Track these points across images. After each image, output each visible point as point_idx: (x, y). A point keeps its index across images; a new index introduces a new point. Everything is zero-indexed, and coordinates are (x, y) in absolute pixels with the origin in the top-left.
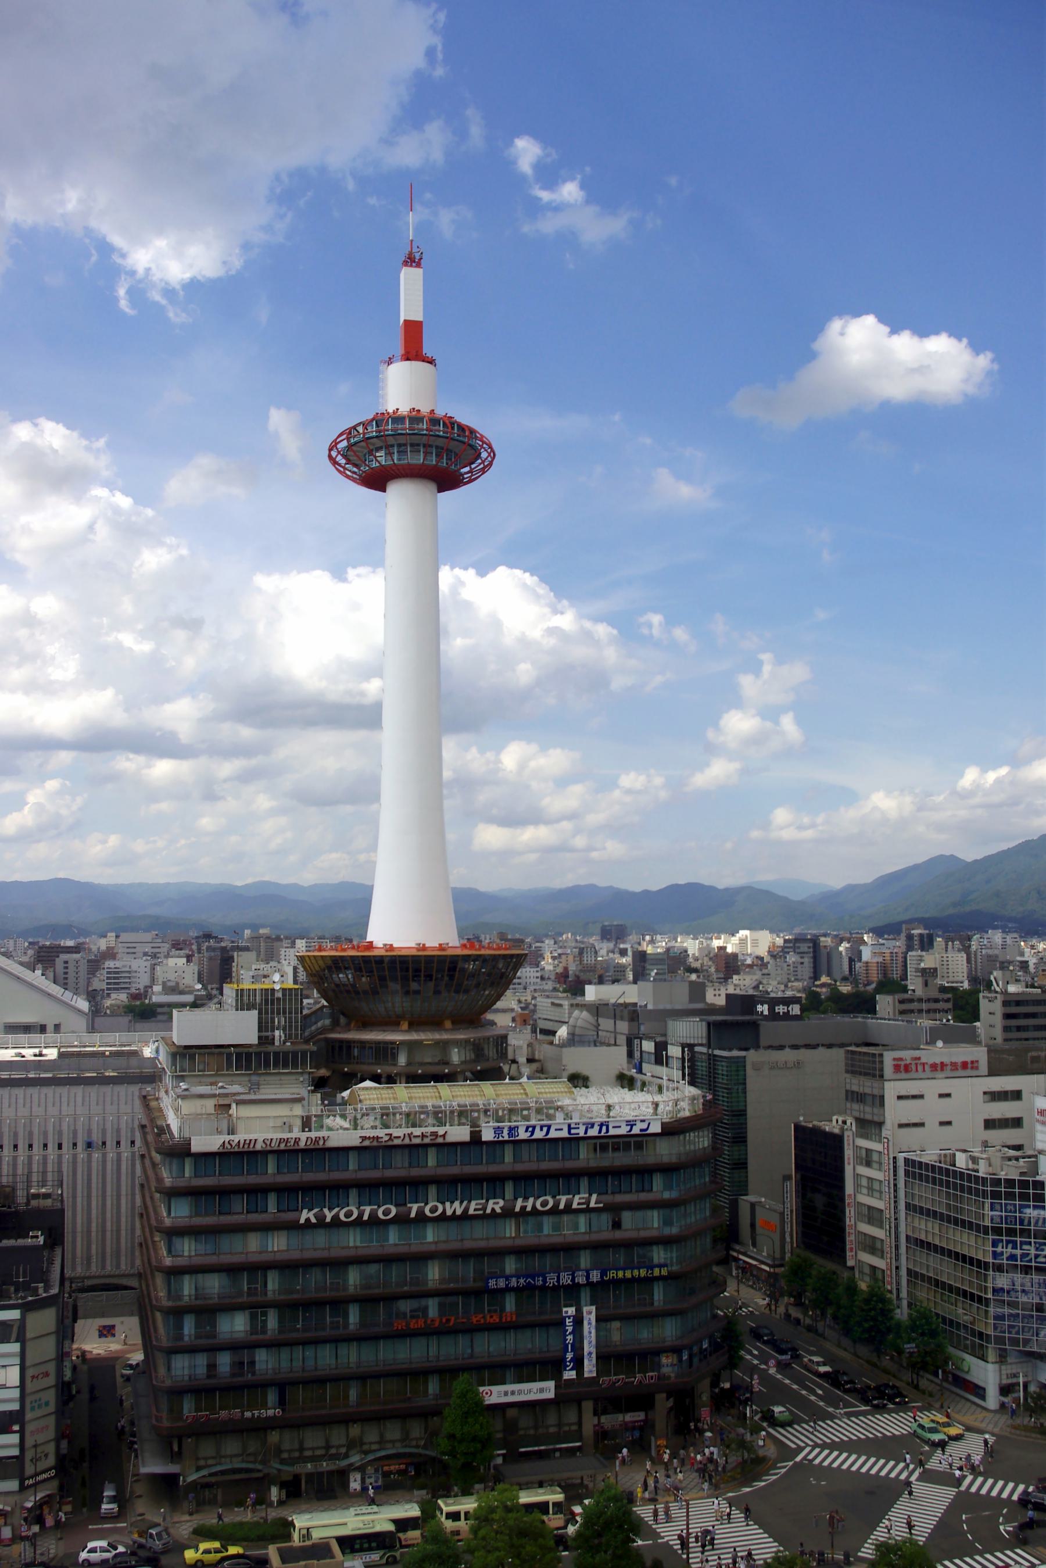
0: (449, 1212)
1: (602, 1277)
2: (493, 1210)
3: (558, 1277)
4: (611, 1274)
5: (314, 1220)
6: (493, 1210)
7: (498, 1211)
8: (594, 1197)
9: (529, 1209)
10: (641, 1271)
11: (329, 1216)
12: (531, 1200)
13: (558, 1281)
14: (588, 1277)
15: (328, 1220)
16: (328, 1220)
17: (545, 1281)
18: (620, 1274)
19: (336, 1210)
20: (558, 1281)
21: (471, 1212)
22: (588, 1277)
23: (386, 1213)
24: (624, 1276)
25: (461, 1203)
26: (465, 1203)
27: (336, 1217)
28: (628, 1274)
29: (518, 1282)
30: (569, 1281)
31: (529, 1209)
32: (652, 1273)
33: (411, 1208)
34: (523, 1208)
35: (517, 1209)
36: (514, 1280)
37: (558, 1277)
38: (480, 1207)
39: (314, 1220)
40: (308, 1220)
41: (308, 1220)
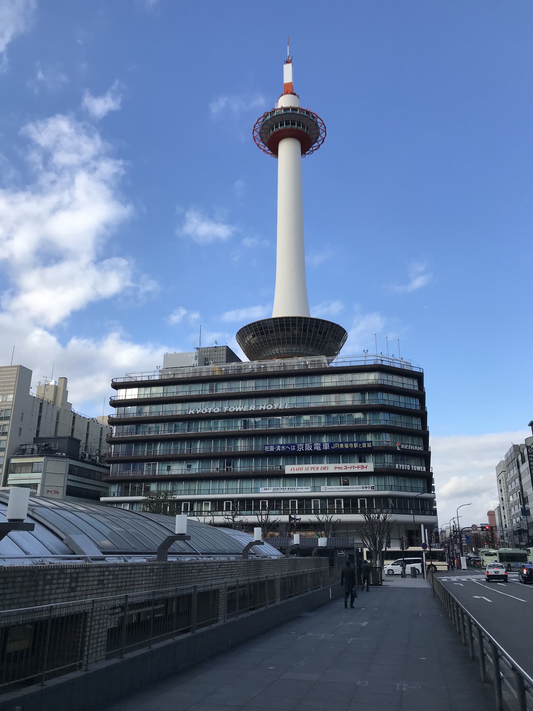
1: (330, 447)
3: (304, 446)
4: (336, 446)
10: (355, 444)
13: (304, 448)
14: (322, 447)
17: (296, 448)
18: (342, 446)
20: (304, 448)
22: (322, 447)
24: (344, 447)
28: (347, 446)
29: (281, 448)
30: (311, 449)
32: (362, 446)
33: (224, 409)
36: (279, 447)
37: (304, 446)
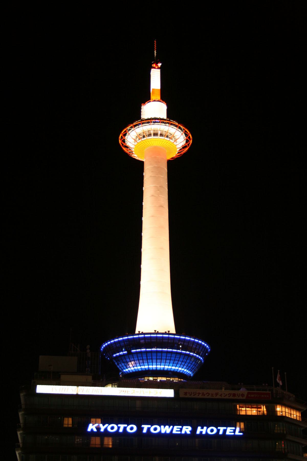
0: (163, 432)
2: (186, 432)
5: (95, 430)
6: (186, 432)
7: (188, 432)
8: (238, 429)
9: (204, 433)
11: (103, 428)
12: (205, 428)
15: (102, 430)
16: (102, 430)
19: (107, 425)
21: (174, 432)
23: (132, 429)
25: (169, 427)
26: (171, 427)
27: (106, 429)
31: (204, 433)
33: (143, 428)
34: (201, 432)
35: (198, 432)
38: (179, 429)
39: (95, 430)
40: (92, 430)
41: (92, 430)
